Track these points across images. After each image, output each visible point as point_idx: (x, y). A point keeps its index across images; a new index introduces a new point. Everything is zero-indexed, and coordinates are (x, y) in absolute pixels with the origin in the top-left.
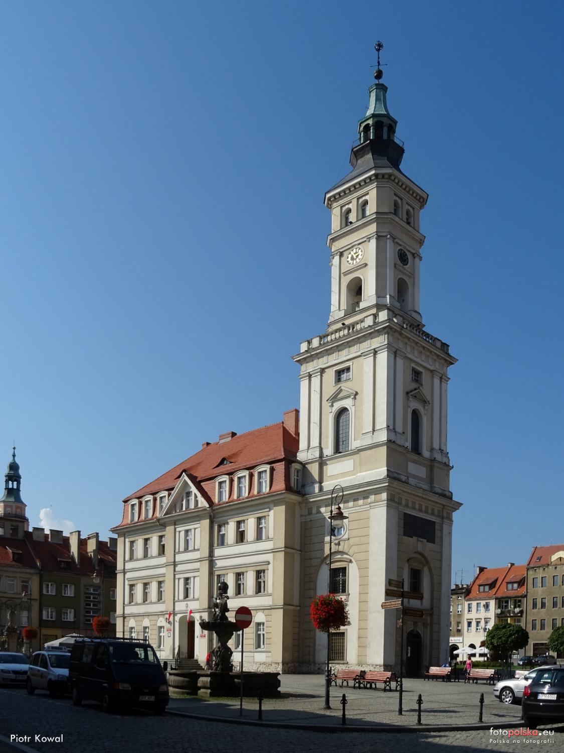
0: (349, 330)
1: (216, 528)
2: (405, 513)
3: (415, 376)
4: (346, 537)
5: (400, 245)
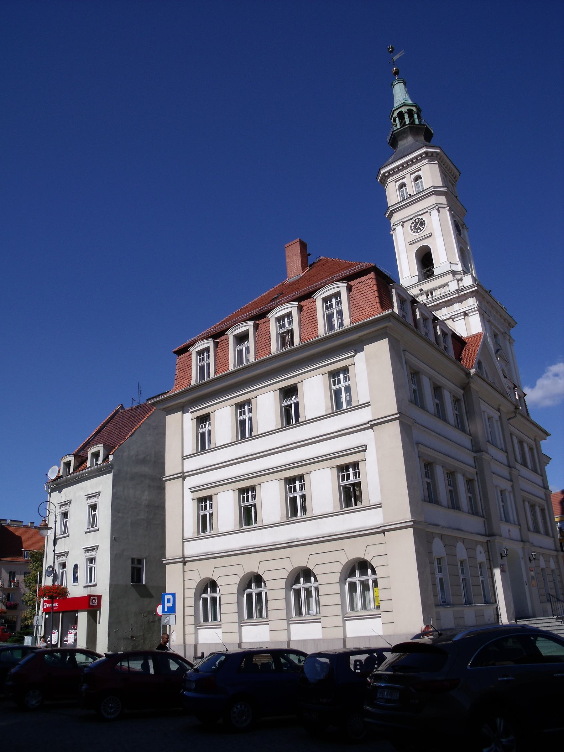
0: (427, 296)
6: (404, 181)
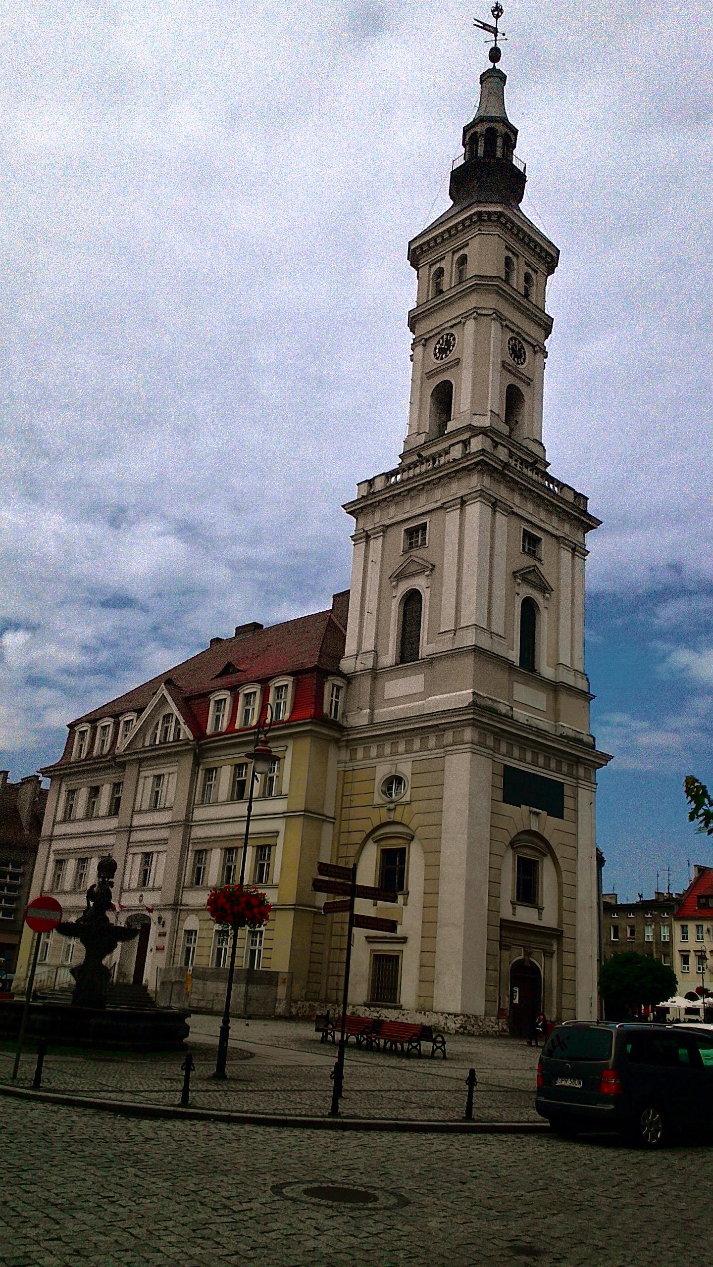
1: (201, 773)
2: (505, 766)
3: (529, 544)
4: (407, 798)
5: (513, 331)
6: (442, 264)
